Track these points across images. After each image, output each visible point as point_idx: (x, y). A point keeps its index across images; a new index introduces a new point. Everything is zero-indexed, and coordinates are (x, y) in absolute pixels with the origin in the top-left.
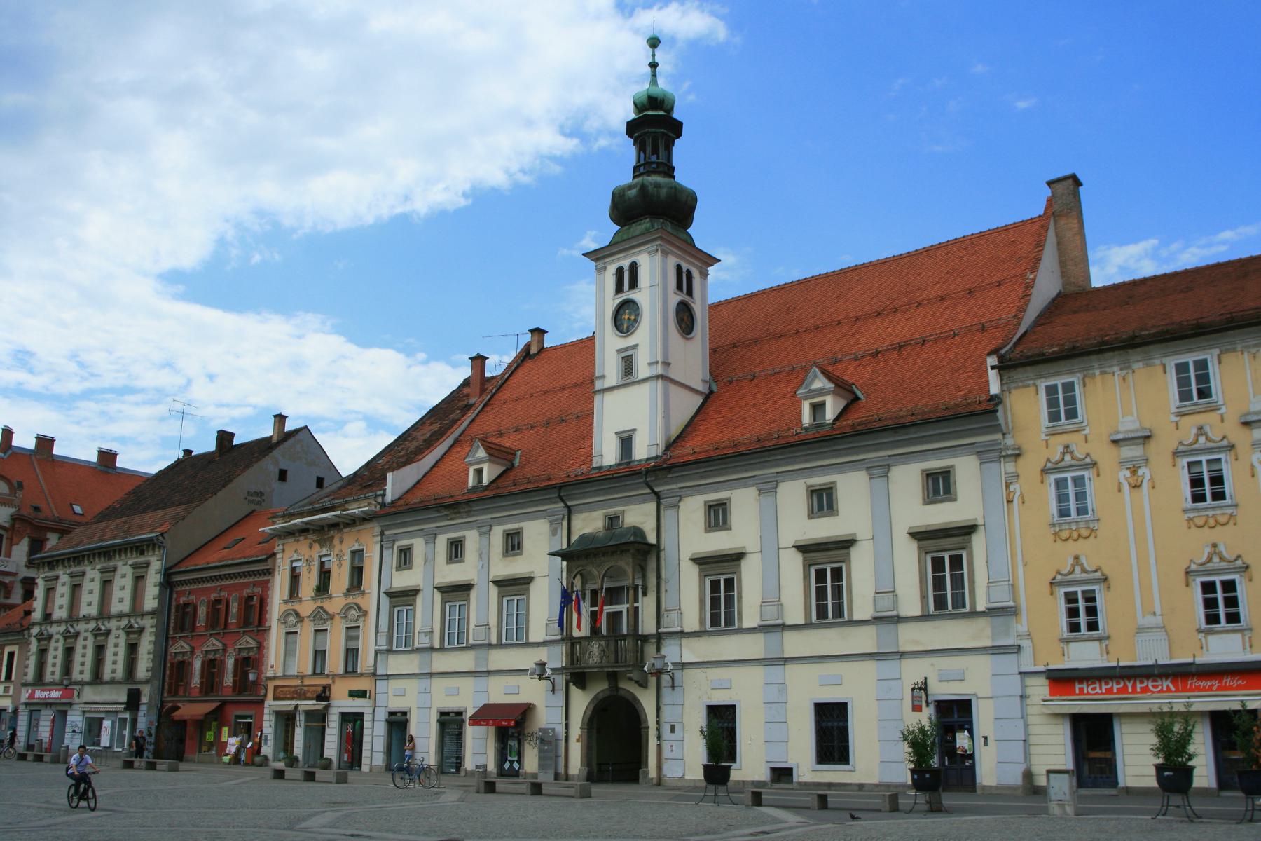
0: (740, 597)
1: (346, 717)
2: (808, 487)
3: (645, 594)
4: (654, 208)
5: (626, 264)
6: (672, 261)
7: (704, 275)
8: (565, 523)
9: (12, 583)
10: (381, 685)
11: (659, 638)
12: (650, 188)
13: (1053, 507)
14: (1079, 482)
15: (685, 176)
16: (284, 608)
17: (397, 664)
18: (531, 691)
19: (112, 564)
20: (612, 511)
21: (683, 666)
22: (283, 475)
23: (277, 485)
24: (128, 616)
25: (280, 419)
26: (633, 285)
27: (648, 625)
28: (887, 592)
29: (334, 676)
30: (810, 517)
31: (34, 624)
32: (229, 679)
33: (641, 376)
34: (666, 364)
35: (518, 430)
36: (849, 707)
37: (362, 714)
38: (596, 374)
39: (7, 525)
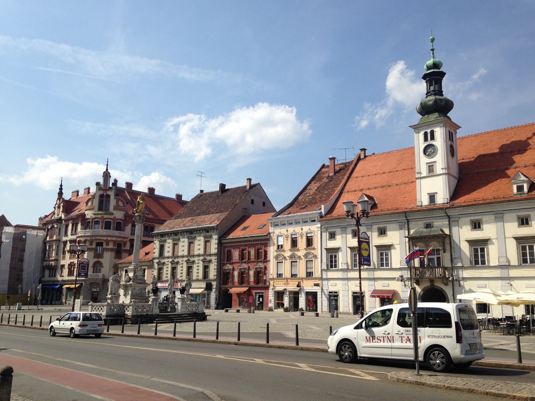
0: (488, 255)
1: (307, 294)
2: (518, 216)
3: (444, 252)
5: (429, 131)
6: (448, 129)
7: (456, 133)
8: (406, 226)
9: (126, 241)
10: (325, 282)
11: (453, 268)
12: (438, 101)
16: (276, 254)
17: (331, 274)
18: (396, 286)
19: (193, 235)
20: (428, 221)
21: (464, 279)
22: (252, 202)
23: (250, 205)
24: (203, 255)
25: (250, 180)
26: (433, 138)
27: (447, 263)
29: (302, 279)
30: (519, 227)
31: (154, 258)
32: (252, 279)
33: (438, 173)
35: (369, 189)
37: (317, 292)
38: (417, 171)
39: (123, 219)
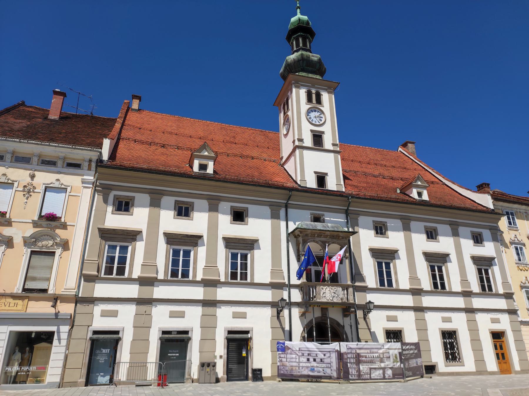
0: (396, 273)
13: (516, 257)
14: (521, 249)
17: (101, 290)
36: (230, 330)
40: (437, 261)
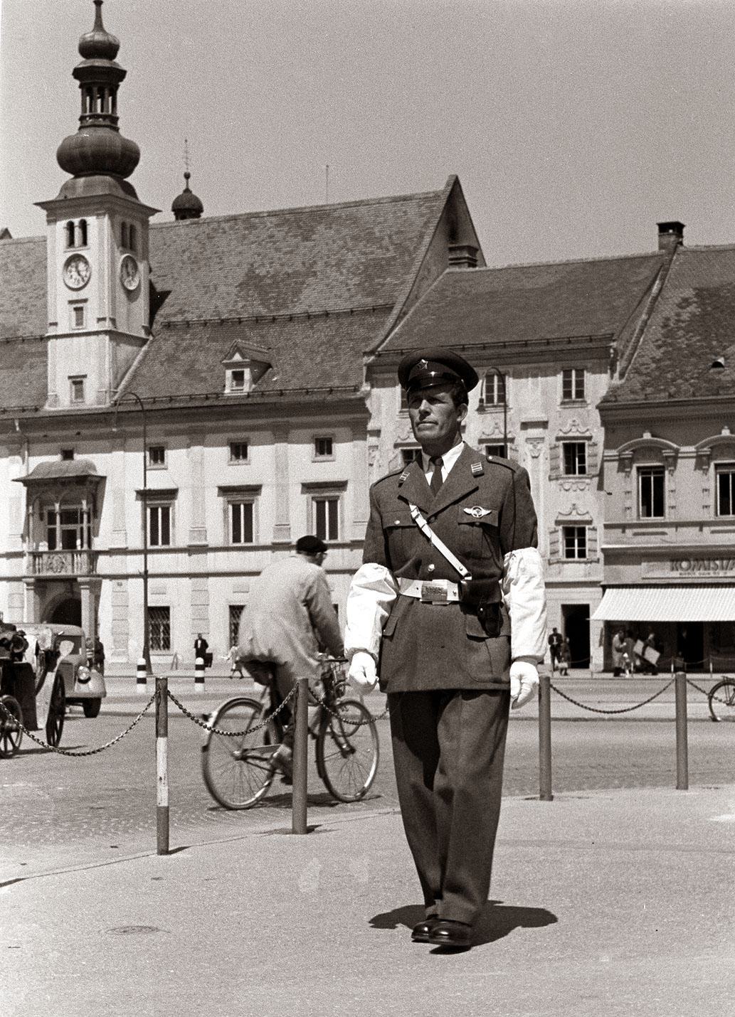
4: (99, 163)
5: (76, 221)
6: (119, 219)
15: (128, 130)
28: (282, 527)
34: (113, 321)
40: (240, 499)
